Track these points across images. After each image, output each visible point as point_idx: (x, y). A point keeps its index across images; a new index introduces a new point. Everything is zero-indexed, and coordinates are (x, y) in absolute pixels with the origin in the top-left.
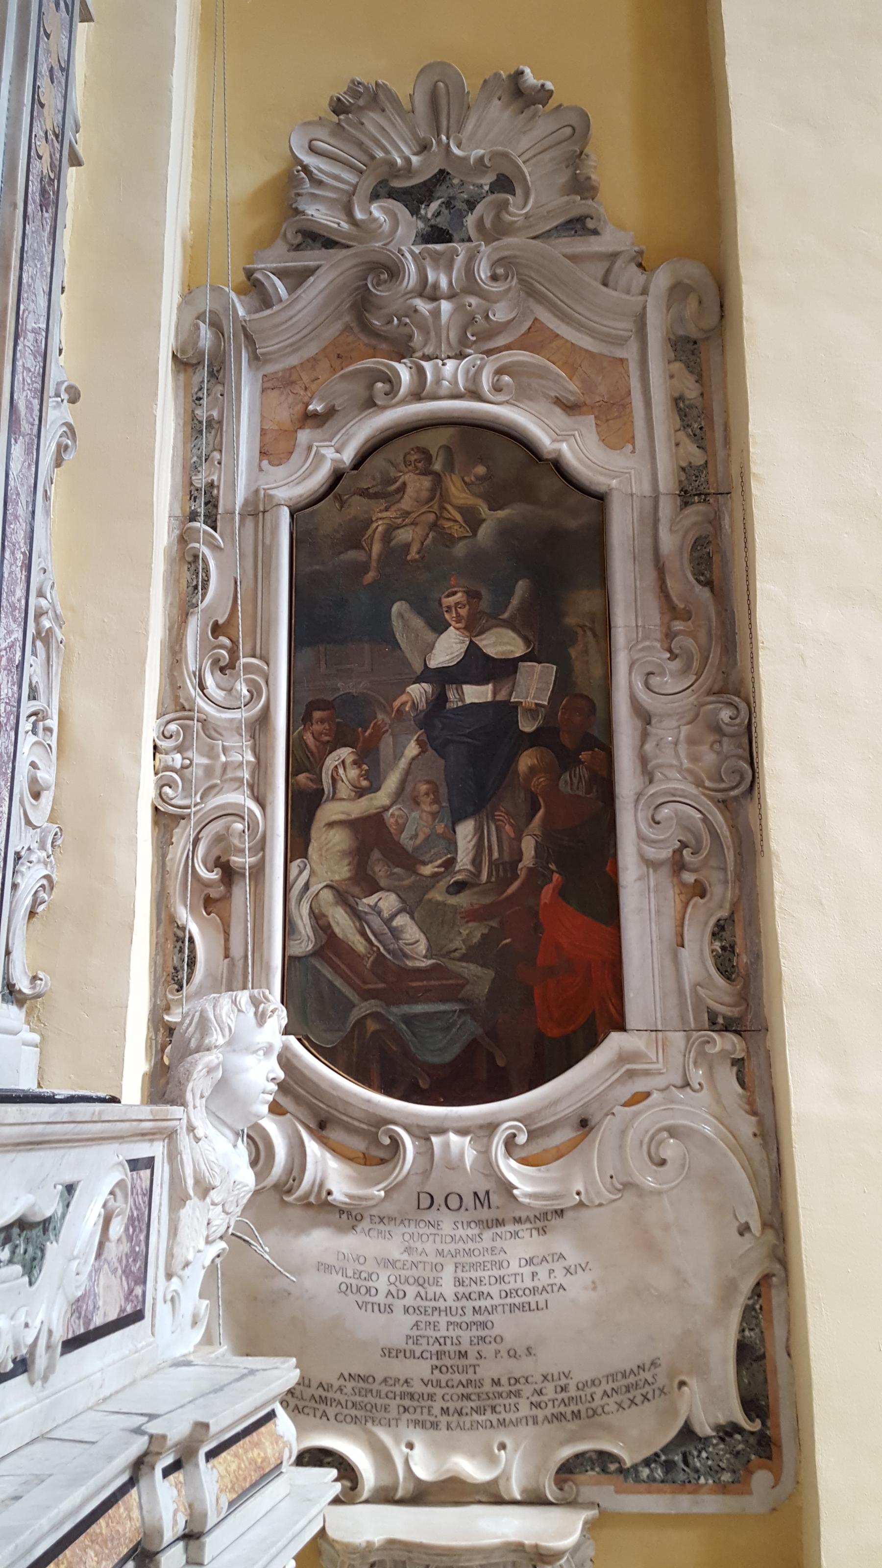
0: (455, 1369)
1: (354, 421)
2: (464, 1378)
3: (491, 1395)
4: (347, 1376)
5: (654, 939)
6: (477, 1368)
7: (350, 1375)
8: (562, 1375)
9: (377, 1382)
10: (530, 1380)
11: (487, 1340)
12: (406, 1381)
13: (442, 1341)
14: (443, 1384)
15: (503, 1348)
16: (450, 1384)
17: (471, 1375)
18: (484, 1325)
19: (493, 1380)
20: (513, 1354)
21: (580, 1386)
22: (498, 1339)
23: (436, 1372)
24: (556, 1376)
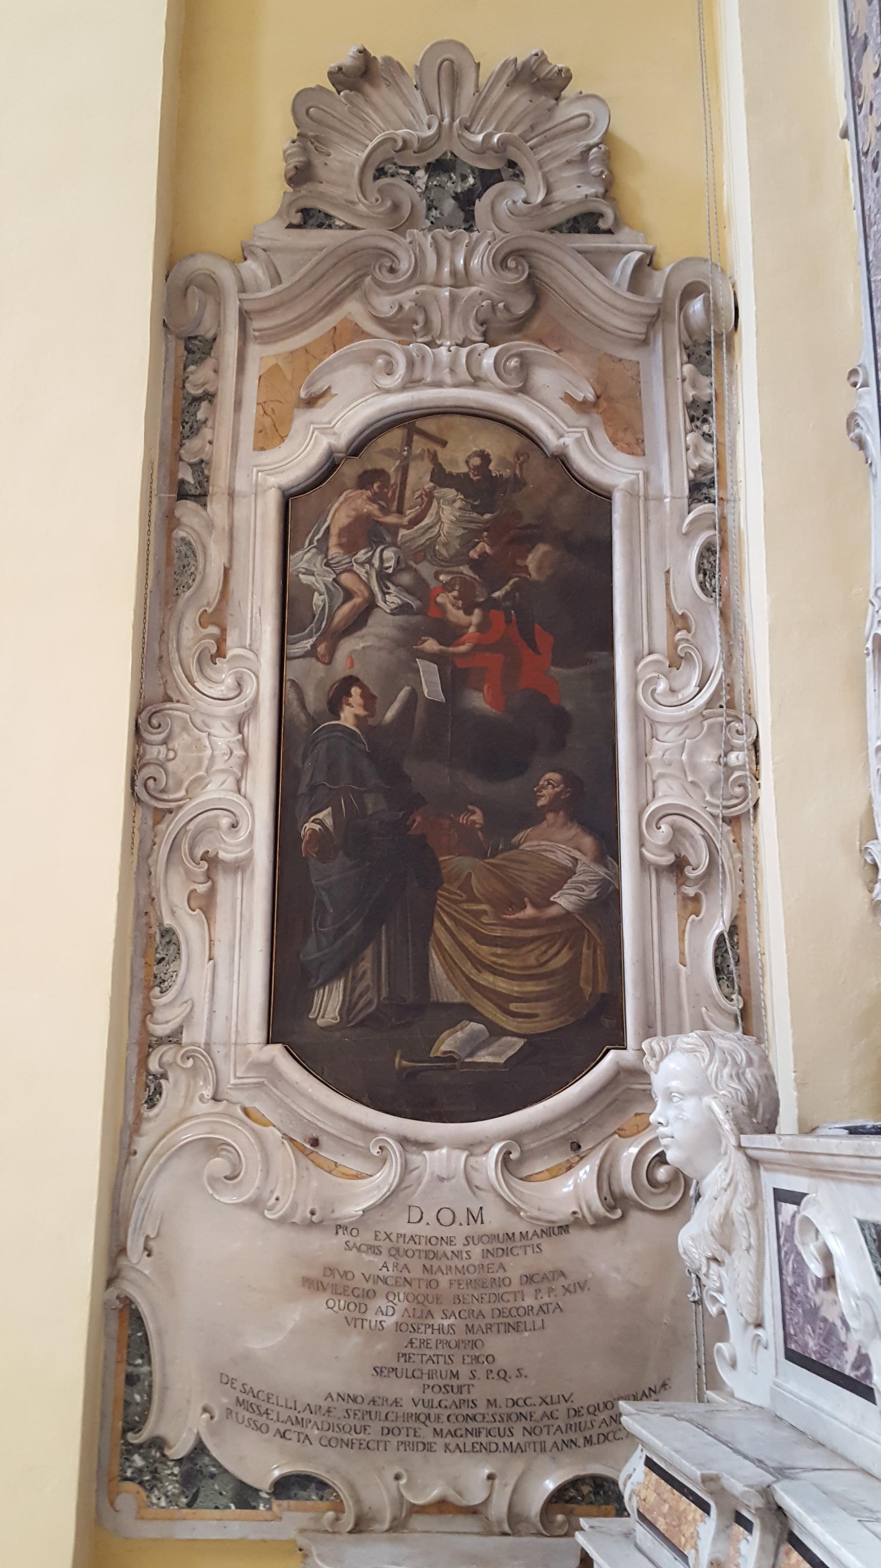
0: (449, 1389)
1: (360, 401)
2: (457, 1397)
3: (498, 1418)
4: (335, 1396)
5: (837, 1159)
6: (471, 1387)
7: (339, 1395)
8: (561, 1398)
9: (366, 1402)
10: (528, 1402)
11: (481, 1360)
12: (396, 1401)
13: (435, 1359)
14: (436, 1404)
15: (495, 1367)
16: (443, 1404)
17: (465, 1396)
18: (474, 1344)
19: (488, 1400)
20: (503, 1375)
21: (591, 1410)
22: (490, 1359)
23: (428, 1391)
24: (555, 1399)
